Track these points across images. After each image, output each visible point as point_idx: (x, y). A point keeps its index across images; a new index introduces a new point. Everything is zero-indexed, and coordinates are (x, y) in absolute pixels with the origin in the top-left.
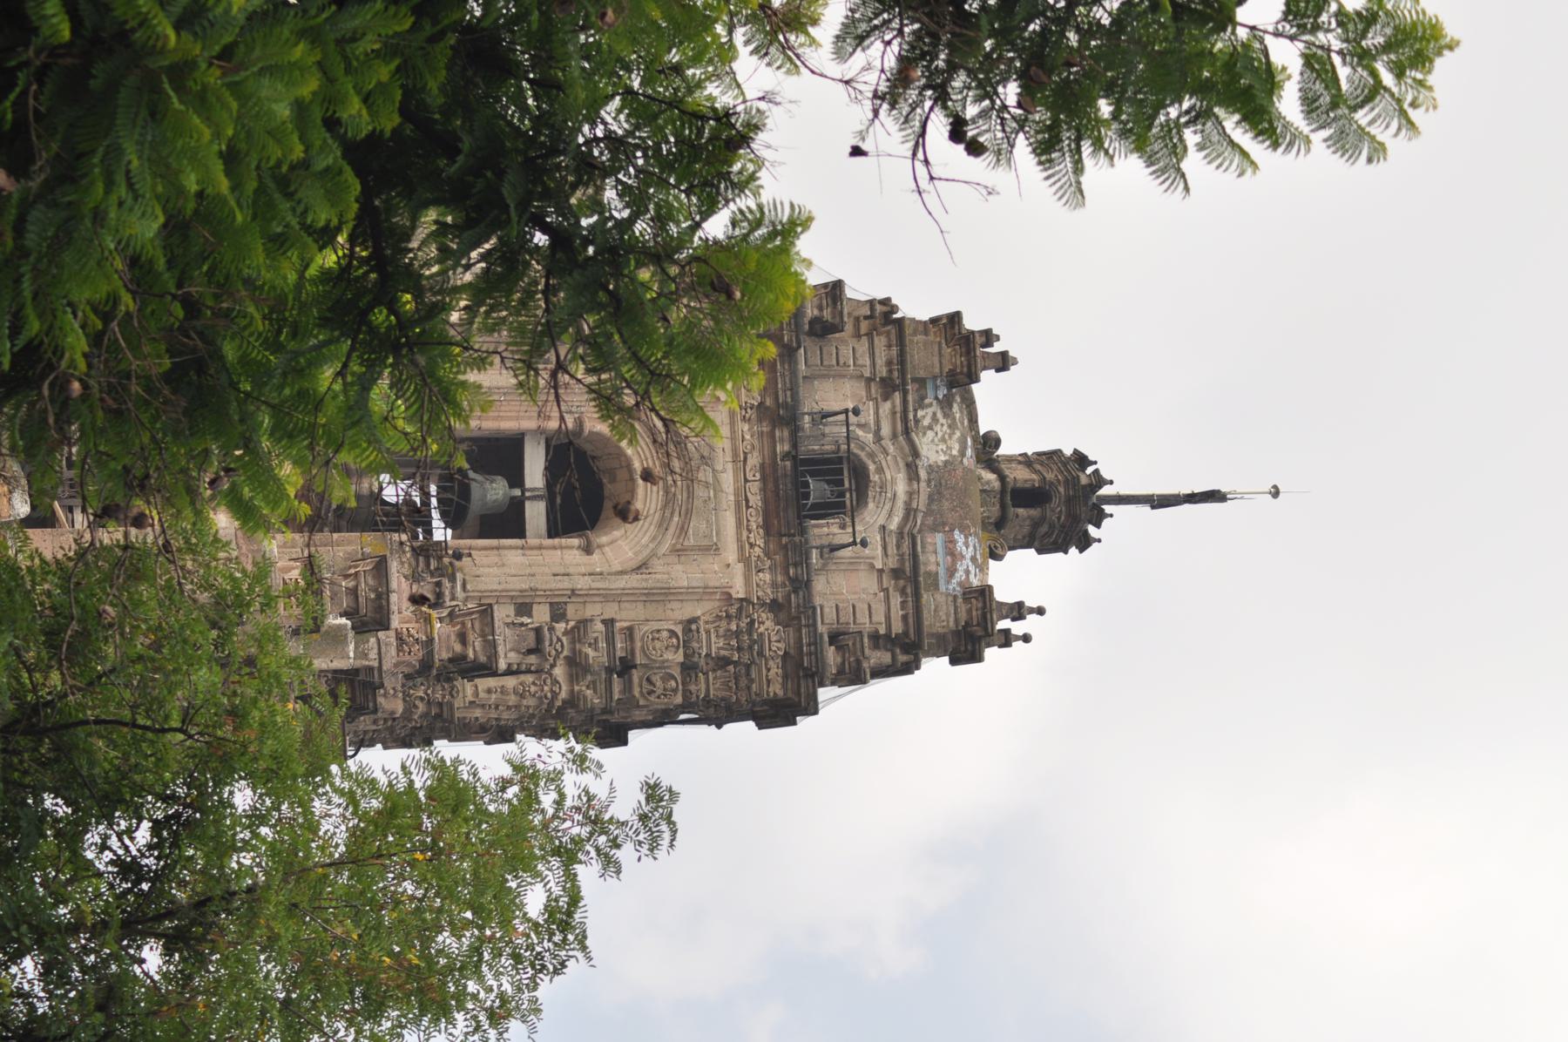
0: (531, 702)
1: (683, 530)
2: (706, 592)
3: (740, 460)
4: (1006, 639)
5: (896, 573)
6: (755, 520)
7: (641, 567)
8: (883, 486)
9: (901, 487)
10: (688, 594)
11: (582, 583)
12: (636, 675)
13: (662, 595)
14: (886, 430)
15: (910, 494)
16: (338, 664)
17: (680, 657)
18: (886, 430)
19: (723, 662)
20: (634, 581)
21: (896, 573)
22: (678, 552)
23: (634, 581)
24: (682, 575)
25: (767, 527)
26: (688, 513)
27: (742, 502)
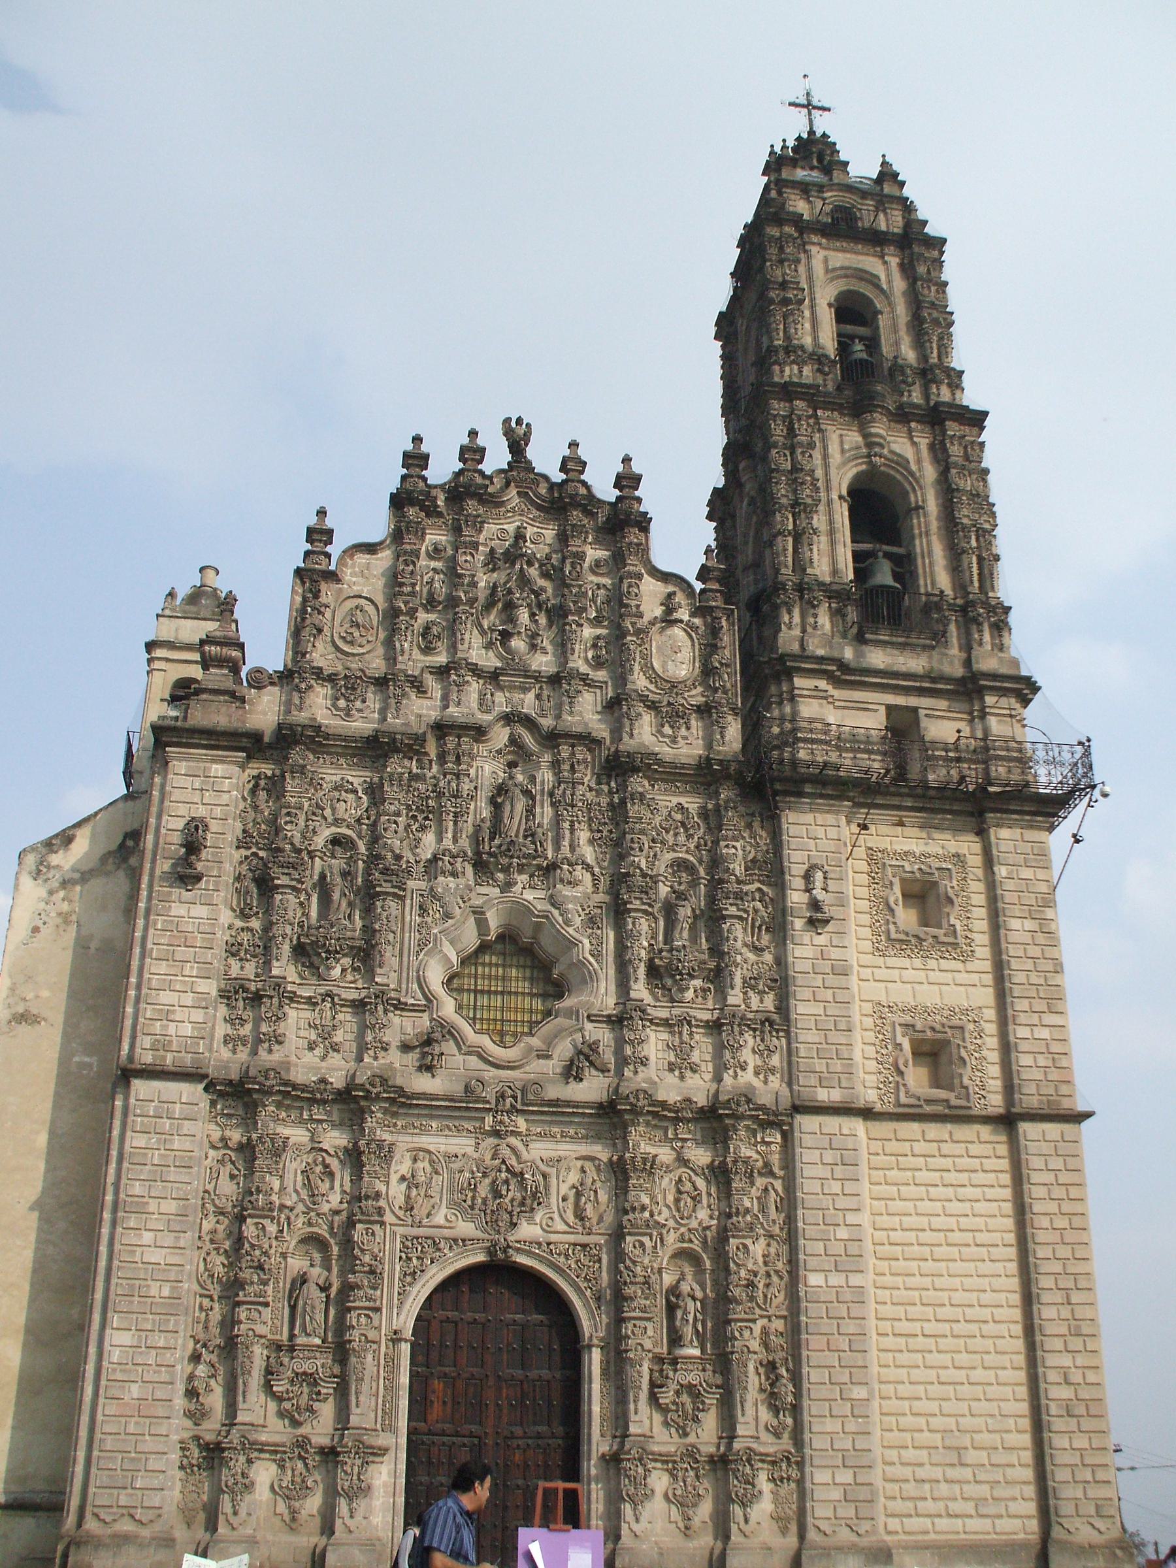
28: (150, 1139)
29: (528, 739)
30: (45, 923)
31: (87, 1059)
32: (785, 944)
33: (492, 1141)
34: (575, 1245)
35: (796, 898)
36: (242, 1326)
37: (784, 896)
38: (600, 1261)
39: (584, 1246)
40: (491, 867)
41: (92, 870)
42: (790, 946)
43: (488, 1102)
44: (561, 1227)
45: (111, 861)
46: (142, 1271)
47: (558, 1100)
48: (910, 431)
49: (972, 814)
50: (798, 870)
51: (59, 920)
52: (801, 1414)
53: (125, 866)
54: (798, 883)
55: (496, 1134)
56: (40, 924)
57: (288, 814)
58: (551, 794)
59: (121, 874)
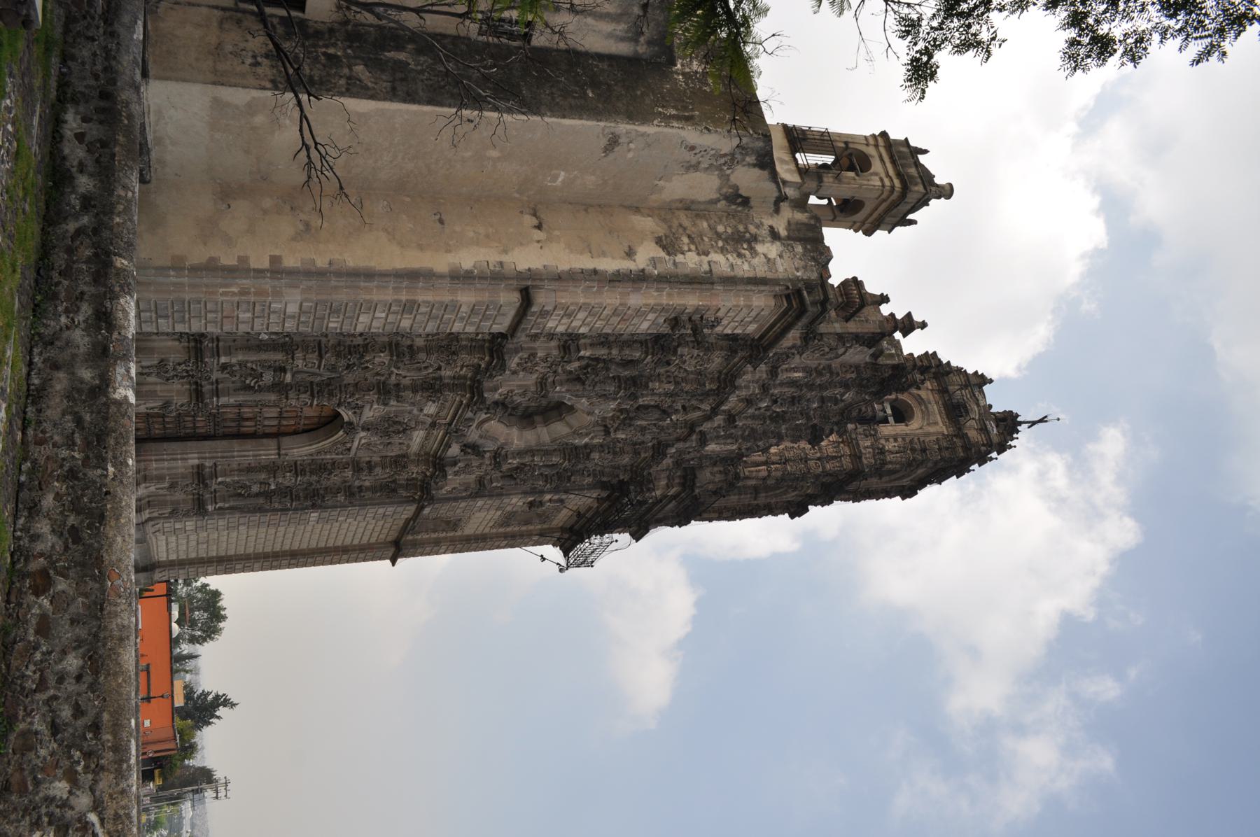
0: (904, 460)
1: (928, 419)
2: (938, 433)
3: (937, 403)
4: (1010, 447)
5: (981, 429)
6: (945, 417)
7: (921, 428)
8: (972, 410)
9: (976, 409)
10: (933, 434)
11: (908, 432)
12: (928, 452)
13: (928, 434)
14: (969, 396)
15: (979, 411)
16: (894, 362)
17: (937, 446)
18: (969, 396)
19: (947, 448)
20: (920, 431)
21: (981, 429)
22: (929, 424)
23: (920, 431)
24: (932, 429)
25: (948, 417)
26: (929, 415)
27: (940, 413)
28: (466, 313)
29: (697, 414)
30: (696, 154)
31: (560, 179)
32: (521, 493)
33: (429, 420)
34: (351, 447)
35: (548, 497)
36: (301, 361)
37: (550, 492)
38: (337, 454)
39: (349, 450)
40: (619, 414)
41: (728, 180)
42: (520, 496)
43: (455, 425)
44: (363, 441)
45: (731, 190)
46: (352, 315)
47: (450, 447)
48: (801, 496)
49: (573, 526)
50: (564, 497)
51: (694, 162)
52: (230, 513)
53: (721, 198)
54: (556, 497)
55: (433, 425)
56: (697, 151)
57: (698, 355)
58: (655, 425)
59: (715, 196)
